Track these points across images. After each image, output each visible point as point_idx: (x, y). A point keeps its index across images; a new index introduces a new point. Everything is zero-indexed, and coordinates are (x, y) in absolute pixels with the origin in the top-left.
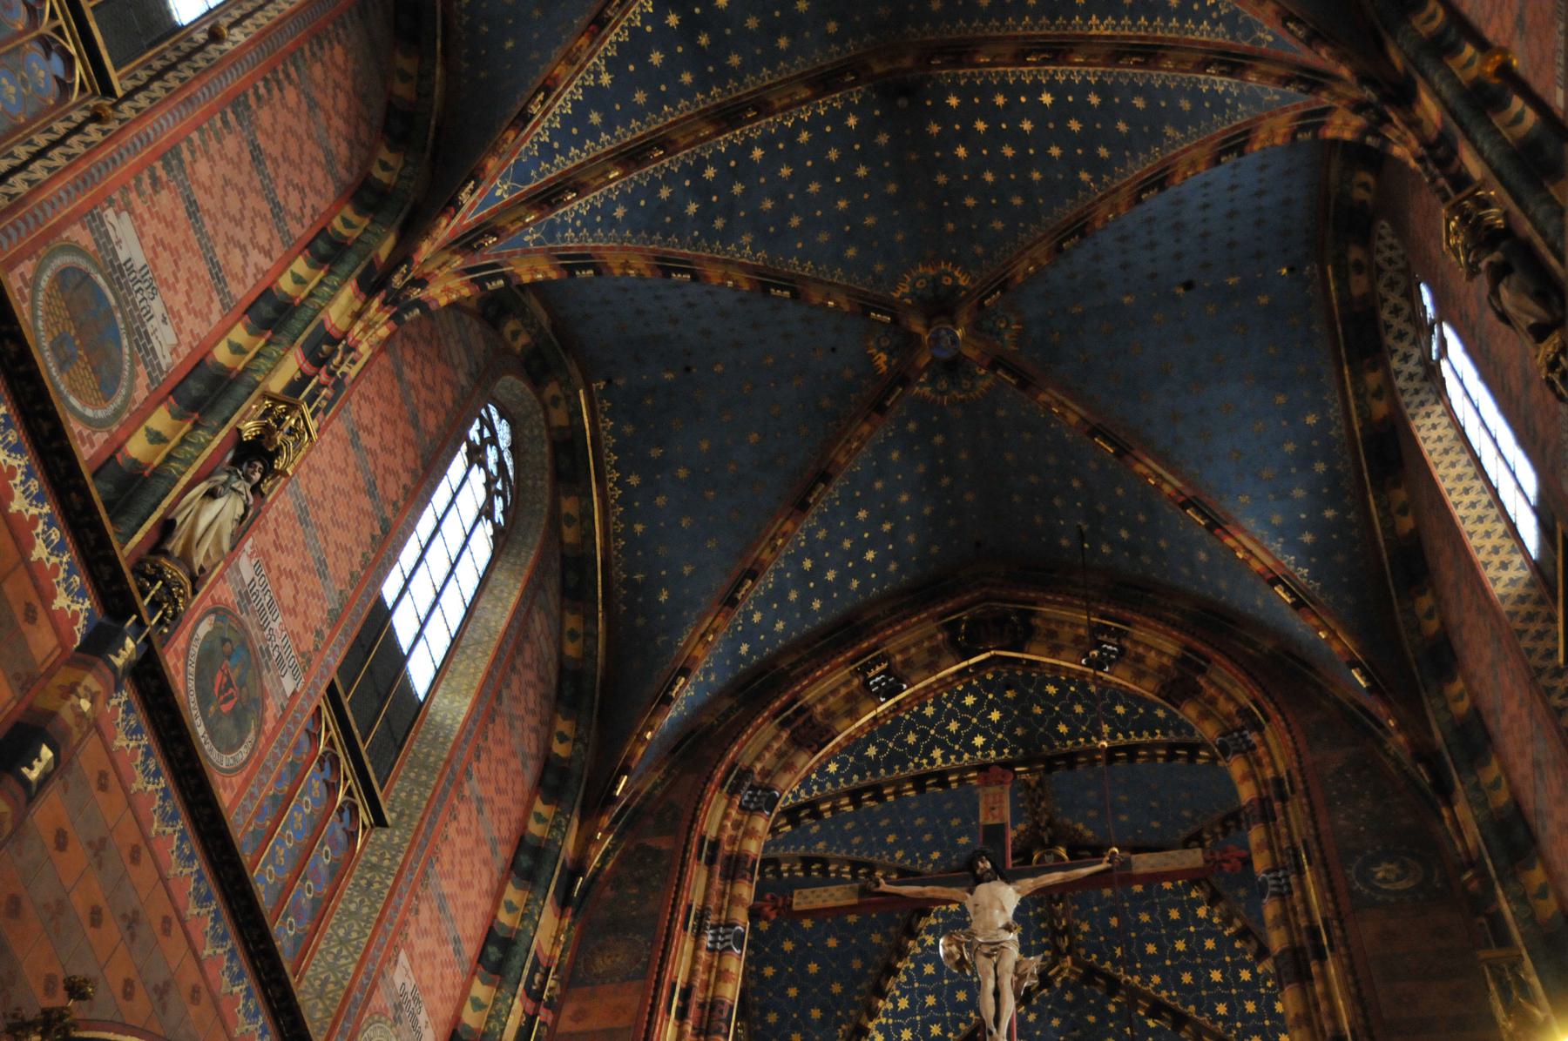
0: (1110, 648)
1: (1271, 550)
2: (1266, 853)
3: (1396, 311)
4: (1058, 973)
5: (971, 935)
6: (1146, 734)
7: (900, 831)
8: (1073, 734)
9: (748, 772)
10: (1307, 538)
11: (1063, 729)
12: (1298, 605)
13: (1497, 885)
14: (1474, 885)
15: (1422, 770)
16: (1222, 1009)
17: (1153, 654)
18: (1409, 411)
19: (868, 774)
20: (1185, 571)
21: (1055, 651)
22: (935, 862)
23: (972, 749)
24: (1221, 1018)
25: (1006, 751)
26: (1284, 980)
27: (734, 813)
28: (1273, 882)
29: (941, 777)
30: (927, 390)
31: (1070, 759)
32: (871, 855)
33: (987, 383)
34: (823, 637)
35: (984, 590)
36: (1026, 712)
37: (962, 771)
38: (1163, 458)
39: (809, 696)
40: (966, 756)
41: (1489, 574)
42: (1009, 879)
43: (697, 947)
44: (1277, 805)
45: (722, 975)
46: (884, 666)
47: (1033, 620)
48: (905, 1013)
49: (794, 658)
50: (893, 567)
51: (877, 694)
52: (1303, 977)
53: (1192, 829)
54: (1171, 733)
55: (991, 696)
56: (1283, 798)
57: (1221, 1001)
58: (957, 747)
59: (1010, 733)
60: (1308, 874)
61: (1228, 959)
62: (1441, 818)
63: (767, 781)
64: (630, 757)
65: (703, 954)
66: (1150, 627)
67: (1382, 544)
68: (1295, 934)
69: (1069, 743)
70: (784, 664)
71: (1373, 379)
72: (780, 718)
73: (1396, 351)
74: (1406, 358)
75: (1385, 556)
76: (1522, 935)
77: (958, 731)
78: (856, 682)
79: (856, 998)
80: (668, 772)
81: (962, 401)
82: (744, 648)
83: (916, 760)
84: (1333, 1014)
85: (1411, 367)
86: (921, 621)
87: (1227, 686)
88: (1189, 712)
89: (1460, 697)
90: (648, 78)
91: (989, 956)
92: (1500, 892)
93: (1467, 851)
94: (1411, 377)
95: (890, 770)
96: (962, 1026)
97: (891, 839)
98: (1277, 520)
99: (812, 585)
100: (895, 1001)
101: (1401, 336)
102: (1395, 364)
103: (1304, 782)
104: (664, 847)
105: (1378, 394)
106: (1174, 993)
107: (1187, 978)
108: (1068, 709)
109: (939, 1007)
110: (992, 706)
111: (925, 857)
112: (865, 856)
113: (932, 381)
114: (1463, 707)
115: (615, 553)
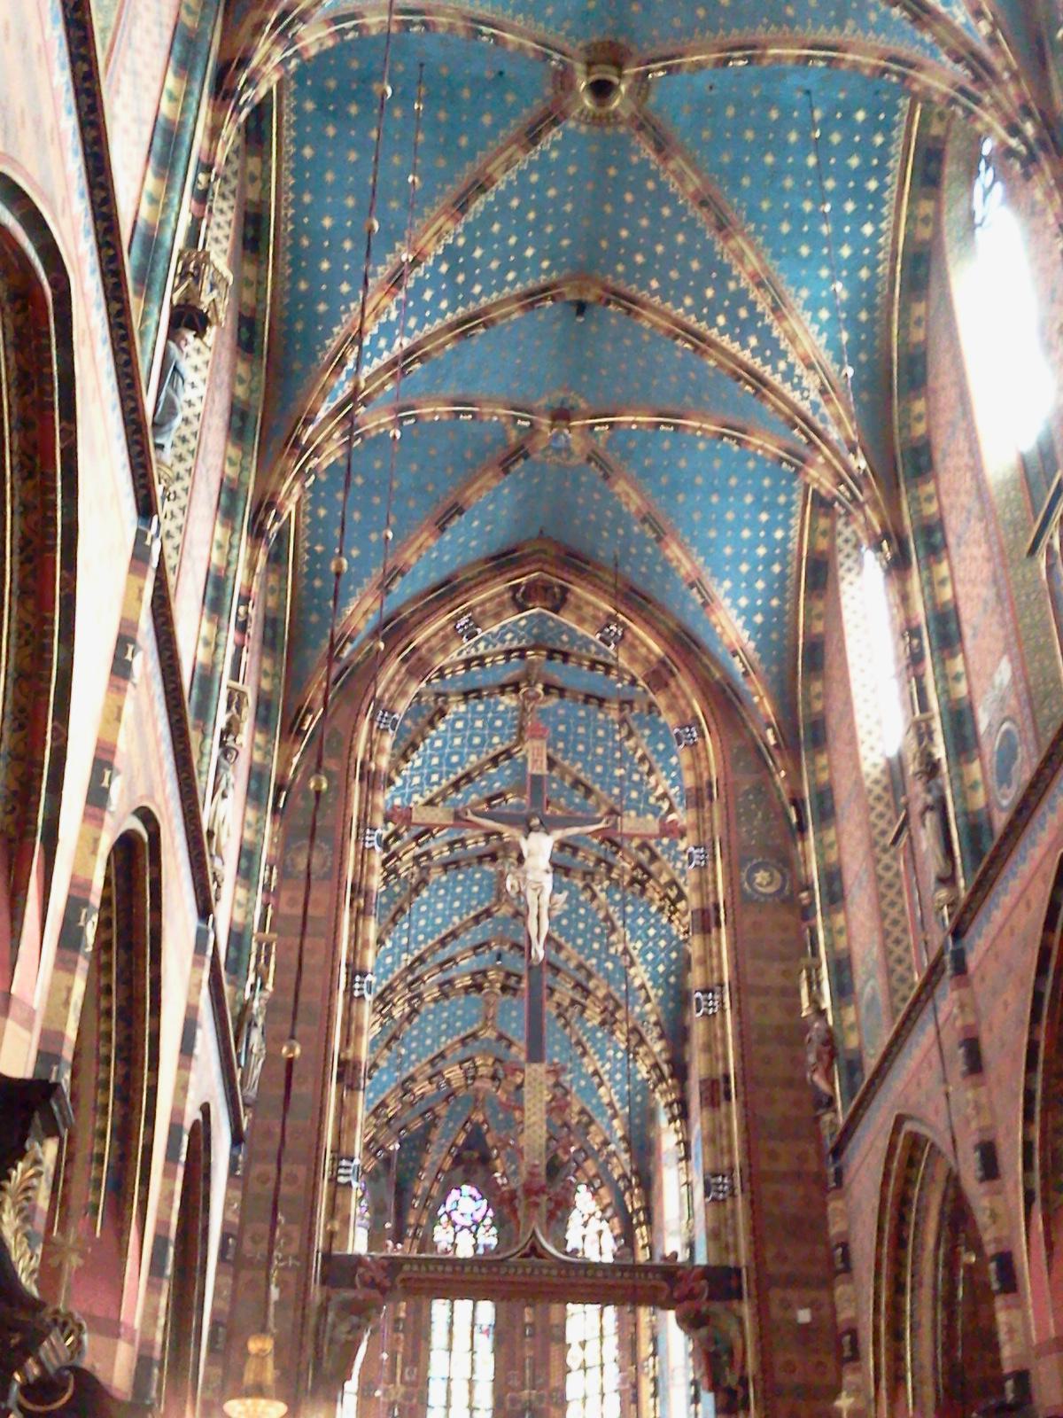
5: (525, 872)
12: (746, 674)
16: (616, 791)
38: (681, 546)
41: (863, 750)
42: (548, 825)
44: (707, 804)
52: (705, 930)
88: (661, 701)
90: (419, 311)
107: (599, 769)
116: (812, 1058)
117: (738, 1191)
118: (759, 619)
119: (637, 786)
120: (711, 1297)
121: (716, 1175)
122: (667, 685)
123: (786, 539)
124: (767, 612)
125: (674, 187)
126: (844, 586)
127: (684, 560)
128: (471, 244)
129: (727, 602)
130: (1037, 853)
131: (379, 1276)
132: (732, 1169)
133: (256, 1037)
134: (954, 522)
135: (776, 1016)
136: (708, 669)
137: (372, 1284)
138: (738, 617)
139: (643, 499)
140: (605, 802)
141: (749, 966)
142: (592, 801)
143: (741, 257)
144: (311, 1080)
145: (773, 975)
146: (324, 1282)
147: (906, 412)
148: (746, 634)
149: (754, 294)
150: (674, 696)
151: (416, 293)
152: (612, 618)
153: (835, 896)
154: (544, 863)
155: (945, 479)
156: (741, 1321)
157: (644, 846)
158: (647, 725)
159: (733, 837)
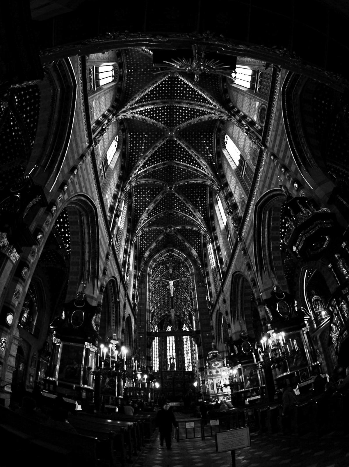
42: (172, 280)
119: (185, 275)
125: (181, 198)
128: (156, 207)
130: (230, 275)
133: (137, 307)
134: (218, 236)
135: (203, 301)
143: (189, 206)
145: (202, 295)
147: (212, 223)
149: (192, 210)
151: (150, 213)
153: (209, 285)
154: (172, 284)
155: (217, 231)
157: (187, 282)
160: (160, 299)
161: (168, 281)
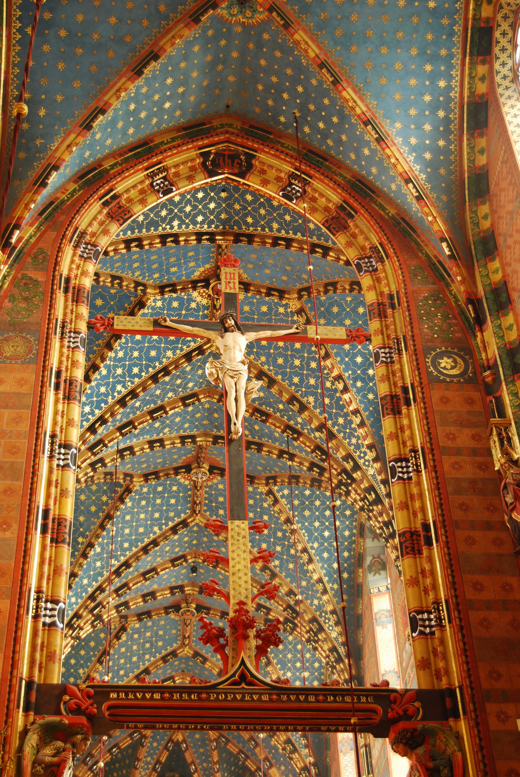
0: (297, 188)
1: (408, 160)
2: (380, 337)
3: (504, 34)
4: (209, 348)
6: (299, 234)
7: (142, 262)
8: (254, 225)
9: (83, 234)
10: (428, 156)
11: (250, 220)
12: (419, 198)
13: (504, 383)
14: (489, 380)
15: (471, 309)
16: (296, 380)
17: (324, 200)
18: (502, 100)
19: (136, 231)
20: (353, 156)
21: (265, 183)
22: (155, 279)
23: (195, 223)
24: (294, 384)
25: (213, 226)
26: (385, 412)
27: (76, 259)
28: (383, 355)
29: (176, 237)
30: (225, 12)
31: (250, 238)
32: (123, 272)
33: (261, 17)
34: (131, 150)
35: (227, 136)
36: (230, 206)
37: (188, 235)
39: (120, 188)
40: (191, 227)
42: (241, 328)
43: (62, 347)
44: (389, 311)
45: (74, 364)
46: (164, 174)
47: (254, 162)
48: (121, 360)
49: (112, 162)
50: (178, 113)
51: (158, 191)
52: (396, 412)
53: (306, 285)
54: (315, 238)
55: (212, 194)
56: (393, 307)
57: (296, 376)
58: (187, 221)
59: (217, 217)
60: (404, 356)
61: (306, 355)
62: (476, 337)
63: (93, 240)
64: (21, 218)
65: (65, 350)
66: (324, 183)
67: (466, 168)
68: (393, 387)
69: (251, 229)
70: (107, 165)
71: (481, 70)
72: (103, 200)
73: (499, 58)
74: (504, 64)
75: (466, 175)
76: (513, 414)
77: (190, 212)
78: (147, 182)
79: (95, 348)
80: (38, 228)
81: (244, 23)
82: (87, 154)
83: (164, 226)
84: (412, 437)
85: (505, 71)
86: (188, 149)
87: (365, 230)
89: (496, 271)
91: (232, 377)
92: (504, 387)
93: (488, 360)
94: (505, 77)
95: (148, 230)
96: (150, 370)
97: (136, 265)
98: (413, 141)
99: (131, 119)
100: (116, 353)
101: (503, 50)
102: (497, 66)
103: (407, 302)
104: (40, 279)
105: (482, 79)
106: (271, 368)
107: (280, 361)
108: (256, 210)
109: (140, 358)
110: (212, 199)
111: (150, 276)
112: (119, 274)
113: (229, 7)
114: (497, 277)
115: (12, 76)
116: (509, 499)
117: (446, 622)
118: (428, 156)
120: (423, 718)
121: (420, 612)
122: (345, 228)
123: (449, 88)
124: (436, 151)
126: (505, 109)
127: (359, 102)
129: (399, 140)
131: (86, 704)
132: (437, 602)
136: (384, 209)
137: (77, 711)
138: (410, 153)
139: (318, 46)
140: (287, 391)
141: (441, 431)
142: (274, 390)
144: (15, 527)
146: (26, 710)
148: (417, 167)
150: (354, 236)
152: (292, 176)
154: (239, 354)
156: (458, 737)
158: (323, 315)
159: (416, 331)
160: (127, 565)
161: (211, 334)
